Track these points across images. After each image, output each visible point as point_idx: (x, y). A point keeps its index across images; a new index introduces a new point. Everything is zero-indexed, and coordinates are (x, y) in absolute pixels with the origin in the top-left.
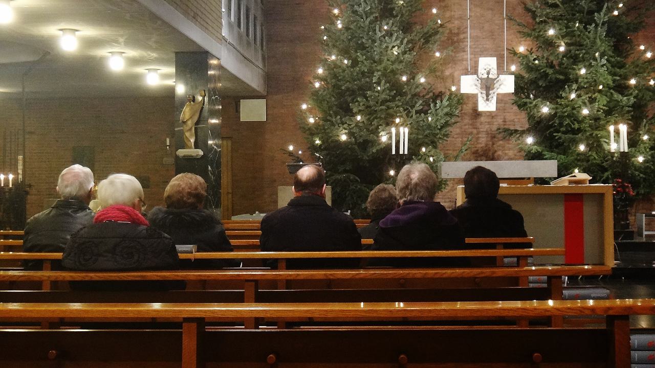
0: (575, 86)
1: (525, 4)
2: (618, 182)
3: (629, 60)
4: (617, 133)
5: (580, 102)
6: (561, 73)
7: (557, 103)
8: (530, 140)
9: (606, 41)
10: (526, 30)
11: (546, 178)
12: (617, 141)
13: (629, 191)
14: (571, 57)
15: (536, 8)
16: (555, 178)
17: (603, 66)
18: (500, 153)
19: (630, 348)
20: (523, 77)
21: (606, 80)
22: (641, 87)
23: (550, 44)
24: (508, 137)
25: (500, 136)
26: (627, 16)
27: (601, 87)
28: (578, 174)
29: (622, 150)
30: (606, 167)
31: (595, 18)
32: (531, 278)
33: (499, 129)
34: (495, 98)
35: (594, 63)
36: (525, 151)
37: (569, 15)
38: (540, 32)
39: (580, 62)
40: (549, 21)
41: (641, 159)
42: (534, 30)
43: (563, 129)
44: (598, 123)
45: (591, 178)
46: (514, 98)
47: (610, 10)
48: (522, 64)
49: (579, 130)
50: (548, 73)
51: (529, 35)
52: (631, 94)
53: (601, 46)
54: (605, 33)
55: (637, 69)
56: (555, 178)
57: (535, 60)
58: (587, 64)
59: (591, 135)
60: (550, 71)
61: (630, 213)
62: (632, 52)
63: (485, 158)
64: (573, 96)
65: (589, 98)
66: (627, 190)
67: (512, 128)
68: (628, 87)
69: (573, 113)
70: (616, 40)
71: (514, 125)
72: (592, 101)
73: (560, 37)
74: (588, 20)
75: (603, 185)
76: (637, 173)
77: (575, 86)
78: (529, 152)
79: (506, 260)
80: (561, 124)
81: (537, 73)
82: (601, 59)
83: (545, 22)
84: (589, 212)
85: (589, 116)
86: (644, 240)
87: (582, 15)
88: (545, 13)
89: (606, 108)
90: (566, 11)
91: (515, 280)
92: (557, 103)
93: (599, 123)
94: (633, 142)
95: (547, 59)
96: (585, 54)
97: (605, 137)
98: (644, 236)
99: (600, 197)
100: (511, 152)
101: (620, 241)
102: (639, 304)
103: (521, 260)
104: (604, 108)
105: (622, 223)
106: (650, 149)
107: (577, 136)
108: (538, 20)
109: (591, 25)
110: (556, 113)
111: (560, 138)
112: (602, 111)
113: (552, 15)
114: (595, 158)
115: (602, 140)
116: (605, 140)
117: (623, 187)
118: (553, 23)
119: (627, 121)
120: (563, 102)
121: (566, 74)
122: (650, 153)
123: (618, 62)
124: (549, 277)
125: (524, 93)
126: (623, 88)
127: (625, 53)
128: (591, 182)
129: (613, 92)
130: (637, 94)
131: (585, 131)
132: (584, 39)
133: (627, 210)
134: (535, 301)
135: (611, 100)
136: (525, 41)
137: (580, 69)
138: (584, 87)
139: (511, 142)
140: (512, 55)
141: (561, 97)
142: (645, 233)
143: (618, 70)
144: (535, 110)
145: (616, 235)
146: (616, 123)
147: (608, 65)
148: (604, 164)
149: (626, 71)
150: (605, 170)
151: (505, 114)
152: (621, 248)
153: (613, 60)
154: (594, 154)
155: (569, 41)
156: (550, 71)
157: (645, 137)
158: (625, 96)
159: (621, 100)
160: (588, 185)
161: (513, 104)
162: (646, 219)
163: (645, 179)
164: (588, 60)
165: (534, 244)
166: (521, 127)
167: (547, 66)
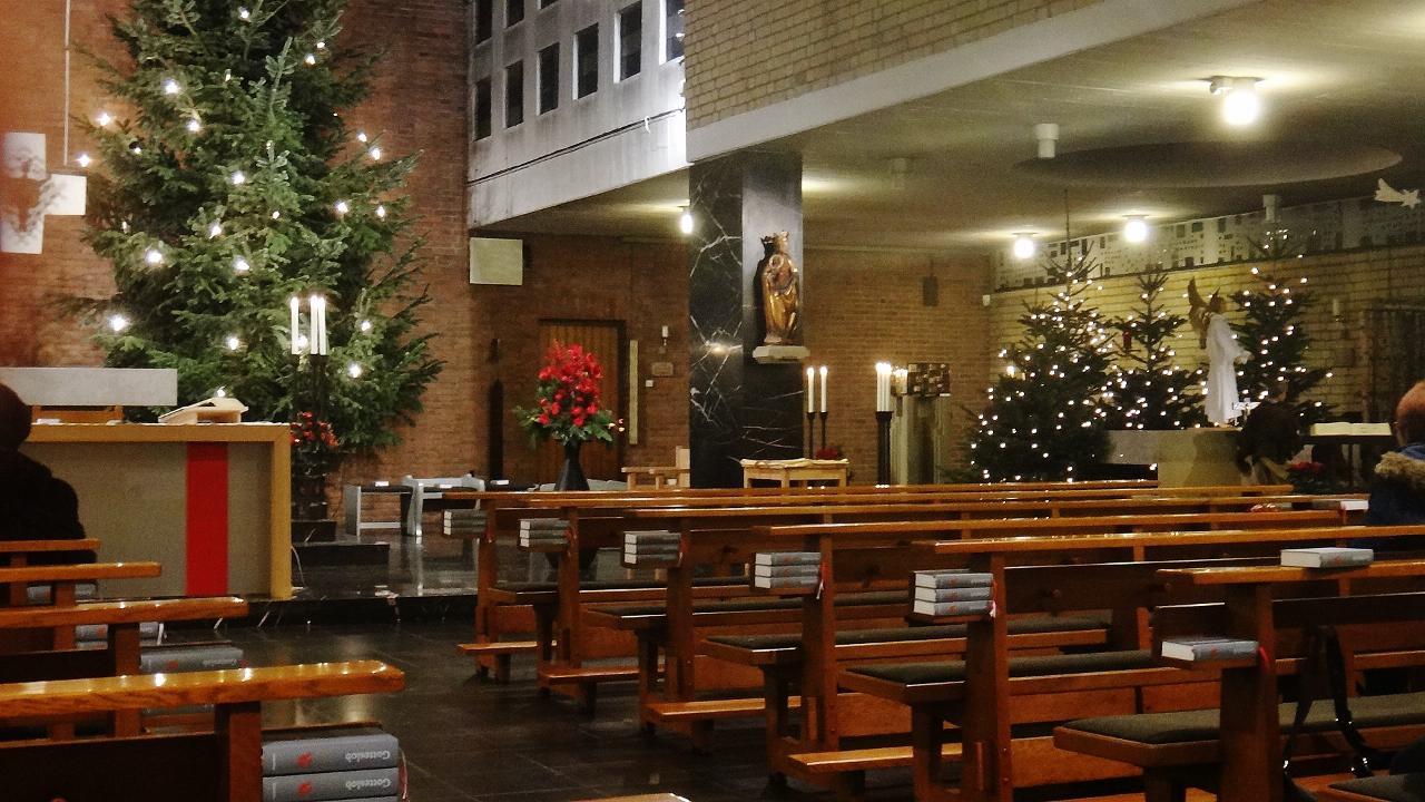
0: (220, 210)
1: (113, 20)
2: (304, 419)
3: (336, 164)
4: (306, 313)
5: (230, 246)
6: (190, 179)
7: (181, 244)
8: (119, 322)
9: (288, 117)
10: (116, 79)
11: (154, 407)
12: (305, 331)
13: (327, 438)
14: (213, 146)
15: (138, 32)
16: (173, 408)
17: (280, 170)
18: (50, 349)
19: (260, 772)
20: (106, 183)
21: (287, 201)
22: (357, 221)
23: (165, 113)
24: (69, 315)
25: (52, 311)
26: (332, 69)
27: (276, 215)
28: (223, 401)
29: (314, 352)
30: (283, 385)
31: (267, 67)
32: (82, 629)
33: (49, 296)
34: (40, 226)
35: (261, 162)
36: (107, 348)
37: (211, 55)
38: (146, 84)
39: (232, 157)
40: (167, 63)
41: (355, 371)
42: (134, 80)
43: (194, 301)
44: (265, 291)
45: (247, 409)
46: (85, 227)
47: (298, 52)
48: (104, 153)
49: (227, 306)
50: (163, 176)
51: (122, 91)
52: (338, 234)
53: (278, 127)
54: (285, 101)
55: (352, 182)
56: (173, 408)
57: (133, 146)
58: (248, 163)
59: (253, 316)
60: (167, 173)
61: (329, 485)
62: (342, 144)
63: (15, 361)
64: (216, 230)
65: (252, 236)
66: (323, 436)
67: (80, 294)
68: (331, 218)
69: (216, 269)
70: (308, 117)
71: (85, 288)
72: (256, 243)
73: (191, 101)
74: (252, 71)
75: (271, 424)
76: (346, 400)
77: (220, 210)
78: (117, 349)
79: (33, 591)
80: (188, 291)
81: (139, 175)
82: (276, 155)
83: (157, 64)
84: (239, 482)
85: (249, 275)
86: (358, 541)
87: (239, 56)
88: (157, 44)
89: (286, 261)
90: (206, 45)
91: (46, 635)
92: (181, 244)
93: (269, 292)
94: (340, 334)
95: (162, 147)
96: (242, 142)
97: (281, 322)
98: (358, 533)
99: (265, 449)
100: (77, 347)
101: (306, 545)
102: (345, 673)
103: (60, 590)
104: (281, 259)
105: (312, 505)
106: (373, 349)
107: (222, 318)
108: (142, 58)
109: (257, 80)
110: (177, 267)
111: (185, 321)
112: (277, 266)
113: (173, 50)
114: (260, 366)
115: (276, 327)
116: (283, 328)
117: (316, 429)
118: (175, 69)
119: (328, 290)
120: (193, 242)
121: (201, 183)
122: (374, 358)
123: (313, 165)
124: (113, 628)
125: (108, 218)
126: (322, 219)
127: (328, 145)
128: (245, 417)
129: (301, 226)
130: (350, 234)
131: (241, 307)
132: (240, 109)
133: (323, 478)
134: (124, 677)
135: (297, 243)
136: (114, 102)
137: (230, 174)
138: (239, 214)
139: (76, 326)
140: (83, 131)
141: (190, 232)
142: (361, 526)
143: (313, 181)
144: (132, 255)
145: (297, 532)
146: (304, 294)
147: (293, 169)
148: (280, 380)
149: (328, 184)
150: (282, 392)
151: (64, 263)
152: (305, 559)
153: (302, 158)
154: (258, 357)
155: (209, 112)
156: (167, 173)
157: (366, 326)
158: (326, 238)
159: (317, 245)
160: (239, 423)
161: (83, 240)
162: (363, 496)
163: (362, 414)
164: (251, 157)
165: (99, 554)
166: (100, 293)
167: (160, 163)
